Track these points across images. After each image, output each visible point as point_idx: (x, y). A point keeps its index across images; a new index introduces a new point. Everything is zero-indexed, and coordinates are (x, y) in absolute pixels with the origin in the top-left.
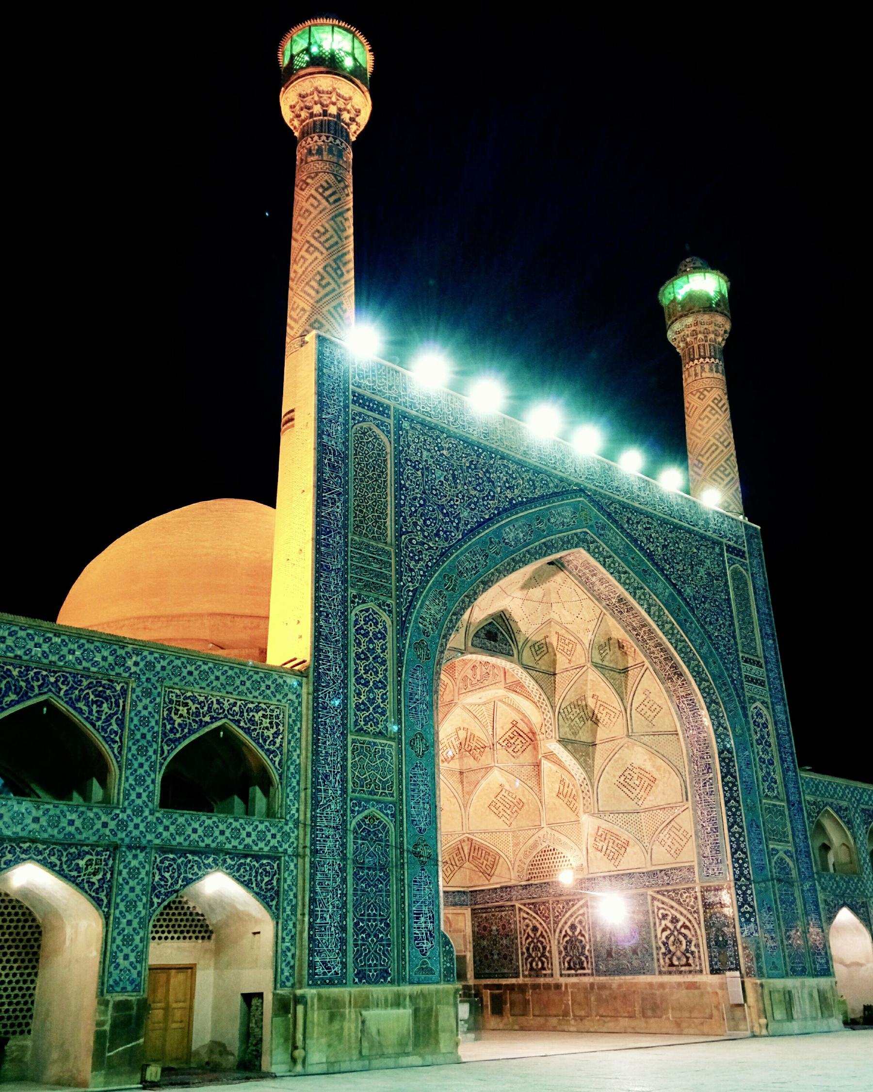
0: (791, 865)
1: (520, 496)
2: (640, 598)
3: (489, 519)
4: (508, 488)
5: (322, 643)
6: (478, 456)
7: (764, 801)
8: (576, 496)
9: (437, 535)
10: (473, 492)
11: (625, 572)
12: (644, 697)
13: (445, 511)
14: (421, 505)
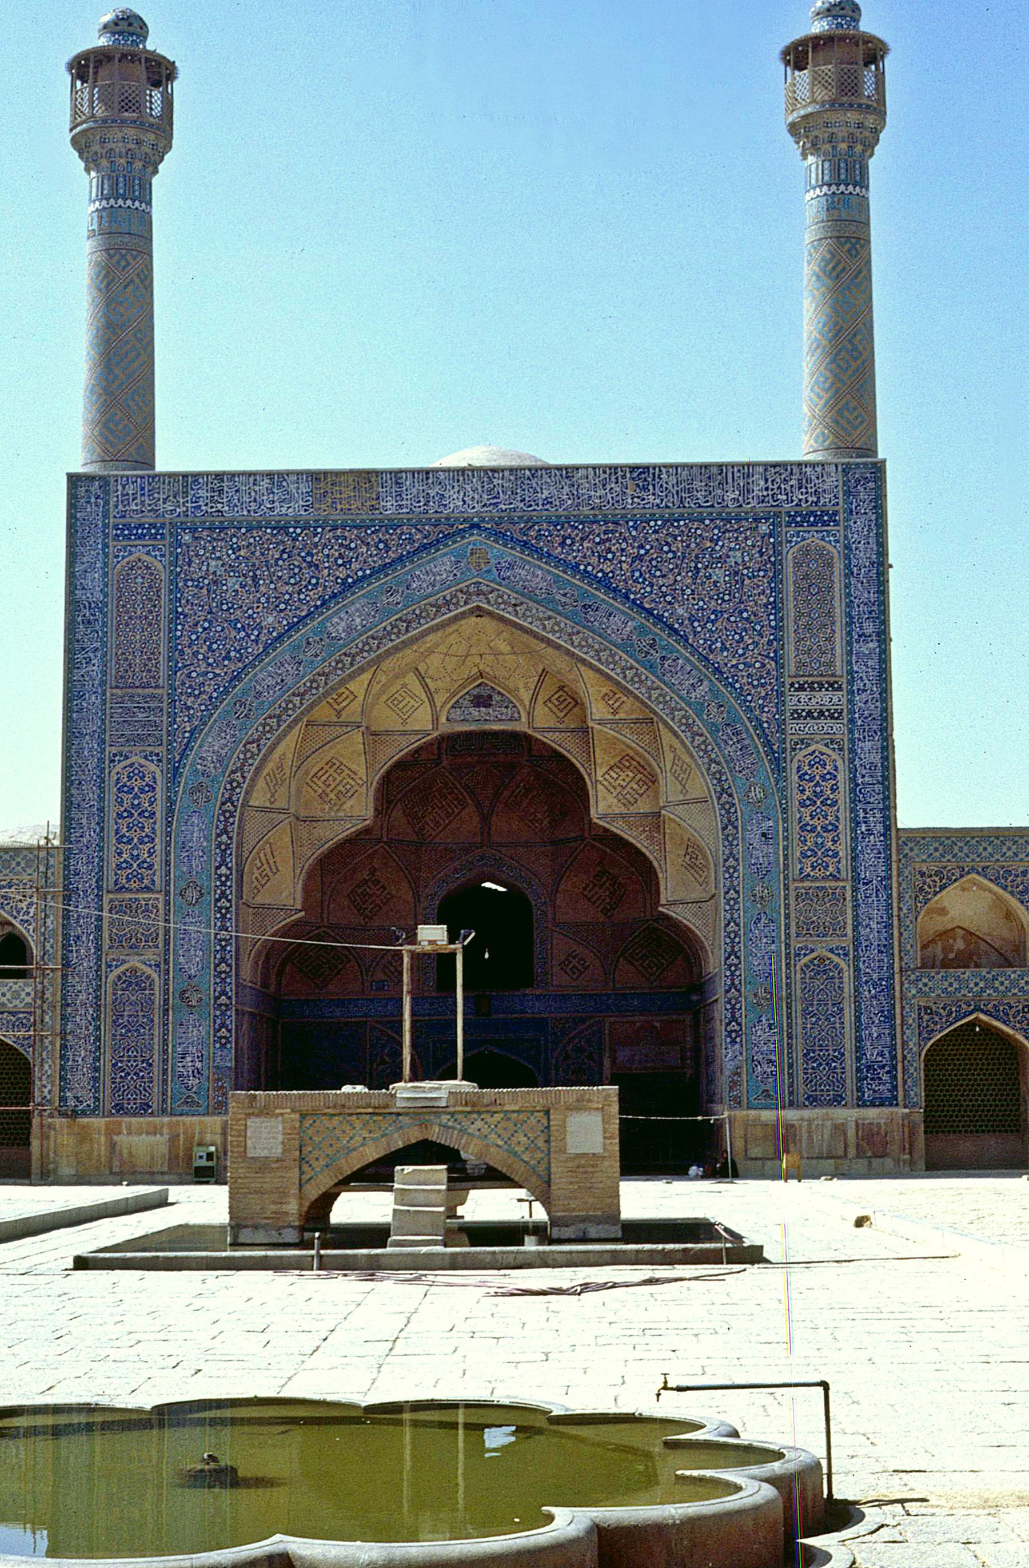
0: (843, 965)
1: (361, 569)
3: (306, 616)
4: (340, 566)
5: (74, 811)
6: (295, 539)
7: (792, 887)
8: (463, 538)
9: (227, 657)
11: (550, 618)
12: (672, 755)
13: (239, 625)
14: (205, 629)
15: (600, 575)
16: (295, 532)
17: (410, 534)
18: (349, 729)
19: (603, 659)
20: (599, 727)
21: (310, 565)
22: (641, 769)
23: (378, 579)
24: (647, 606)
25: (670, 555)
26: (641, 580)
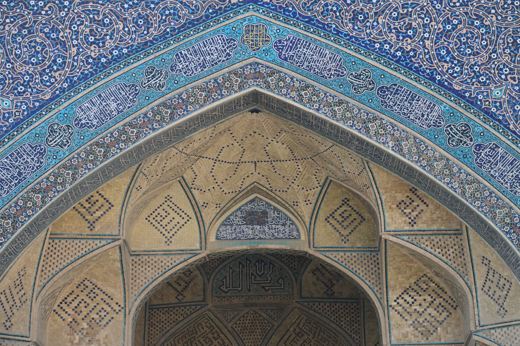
2: (377, 134)
3: (51, 99)
8: (236, 13)
10: (23, 69)
12: (485, 268)
15: (399, 54)
16: (37, 5)
17: (175, 9)
18: (104, 242)
19: (405, 150)
20: (394, 239)
21: (56, 42)
22: (439, 291)
23: (137, 59)
24: (457, 88)
25: (483, 30)
26: (448, 59)
